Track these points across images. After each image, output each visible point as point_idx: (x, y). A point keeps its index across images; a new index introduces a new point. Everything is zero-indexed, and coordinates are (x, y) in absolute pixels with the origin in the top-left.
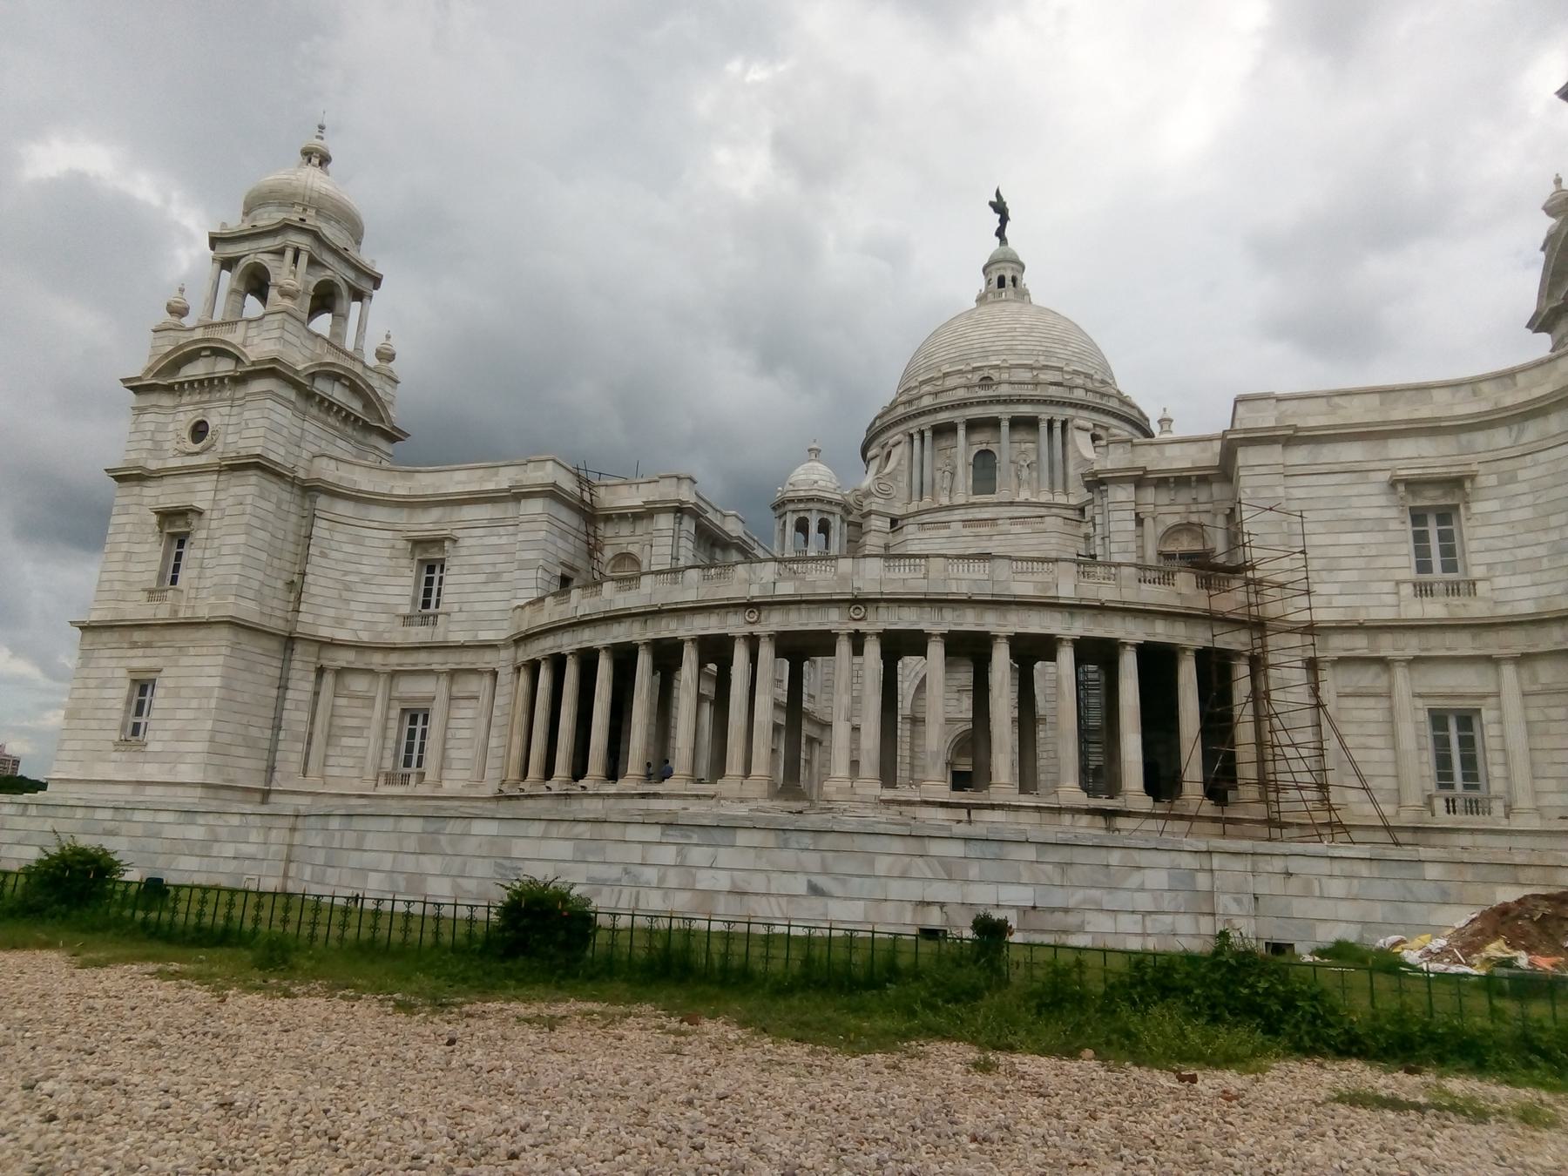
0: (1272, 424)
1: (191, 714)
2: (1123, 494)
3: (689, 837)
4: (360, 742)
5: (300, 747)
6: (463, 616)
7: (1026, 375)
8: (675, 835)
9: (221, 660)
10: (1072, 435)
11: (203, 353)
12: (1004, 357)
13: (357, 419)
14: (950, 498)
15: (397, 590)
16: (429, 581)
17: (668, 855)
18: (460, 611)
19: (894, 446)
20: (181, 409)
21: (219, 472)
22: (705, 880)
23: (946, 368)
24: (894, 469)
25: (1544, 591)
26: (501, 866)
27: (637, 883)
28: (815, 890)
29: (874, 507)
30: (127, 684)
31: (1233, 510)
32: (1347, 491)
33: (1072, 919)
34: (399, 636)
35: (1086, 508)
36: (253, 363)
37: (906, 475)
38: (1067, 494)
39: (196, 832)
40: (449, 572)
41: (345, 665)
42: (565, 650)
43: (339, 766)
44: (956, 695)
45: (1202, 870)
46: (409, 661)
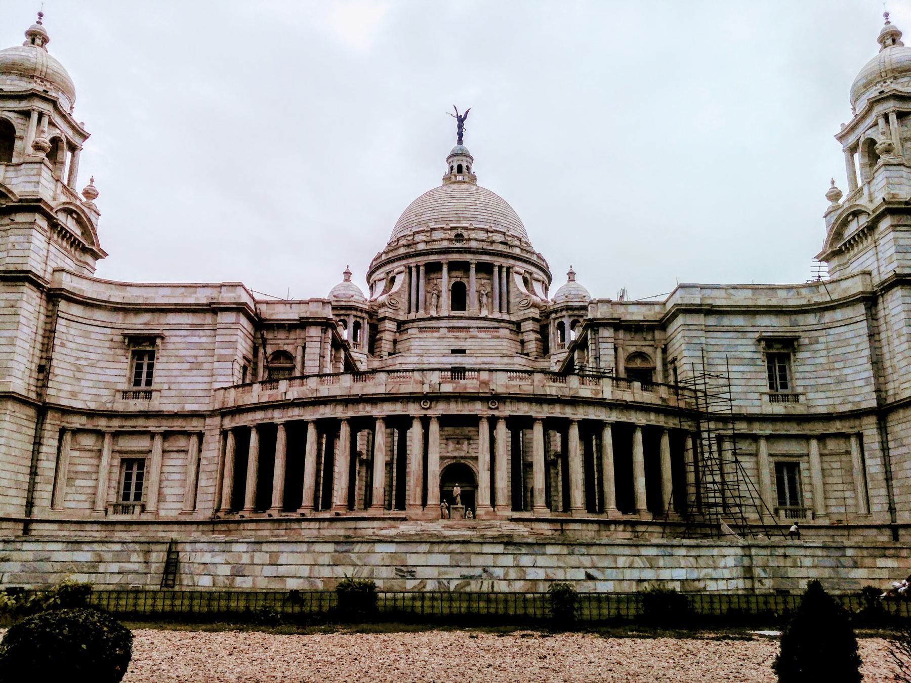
0: (699, 302)
2: (607, 333)
3: (520, 550)
4: (91, 483)
5: (50, 487)
6: (173, 393)
8: (511, 549)
10: (513, 277)
12: (471, 222)
13: (80, 242)
14: (437, 312)
16: (139, 367)
17: (508, 560)
18: (170, 389)
19: (397, 274)
22: (531, 574)
24: (400, 289)
25: (831, 401)
26: (401, 571)
28: (590, 577)
29: (388, 314)
31: (666, 345)
34: (120, 405)
35: (522, 324)
38: (508, 313)
39: (84, 556)
40: (158, 361)
41: (78, 426)
42: (276, 421)
44: (445, 441)
45: (745, 555)
46: (129, 424)
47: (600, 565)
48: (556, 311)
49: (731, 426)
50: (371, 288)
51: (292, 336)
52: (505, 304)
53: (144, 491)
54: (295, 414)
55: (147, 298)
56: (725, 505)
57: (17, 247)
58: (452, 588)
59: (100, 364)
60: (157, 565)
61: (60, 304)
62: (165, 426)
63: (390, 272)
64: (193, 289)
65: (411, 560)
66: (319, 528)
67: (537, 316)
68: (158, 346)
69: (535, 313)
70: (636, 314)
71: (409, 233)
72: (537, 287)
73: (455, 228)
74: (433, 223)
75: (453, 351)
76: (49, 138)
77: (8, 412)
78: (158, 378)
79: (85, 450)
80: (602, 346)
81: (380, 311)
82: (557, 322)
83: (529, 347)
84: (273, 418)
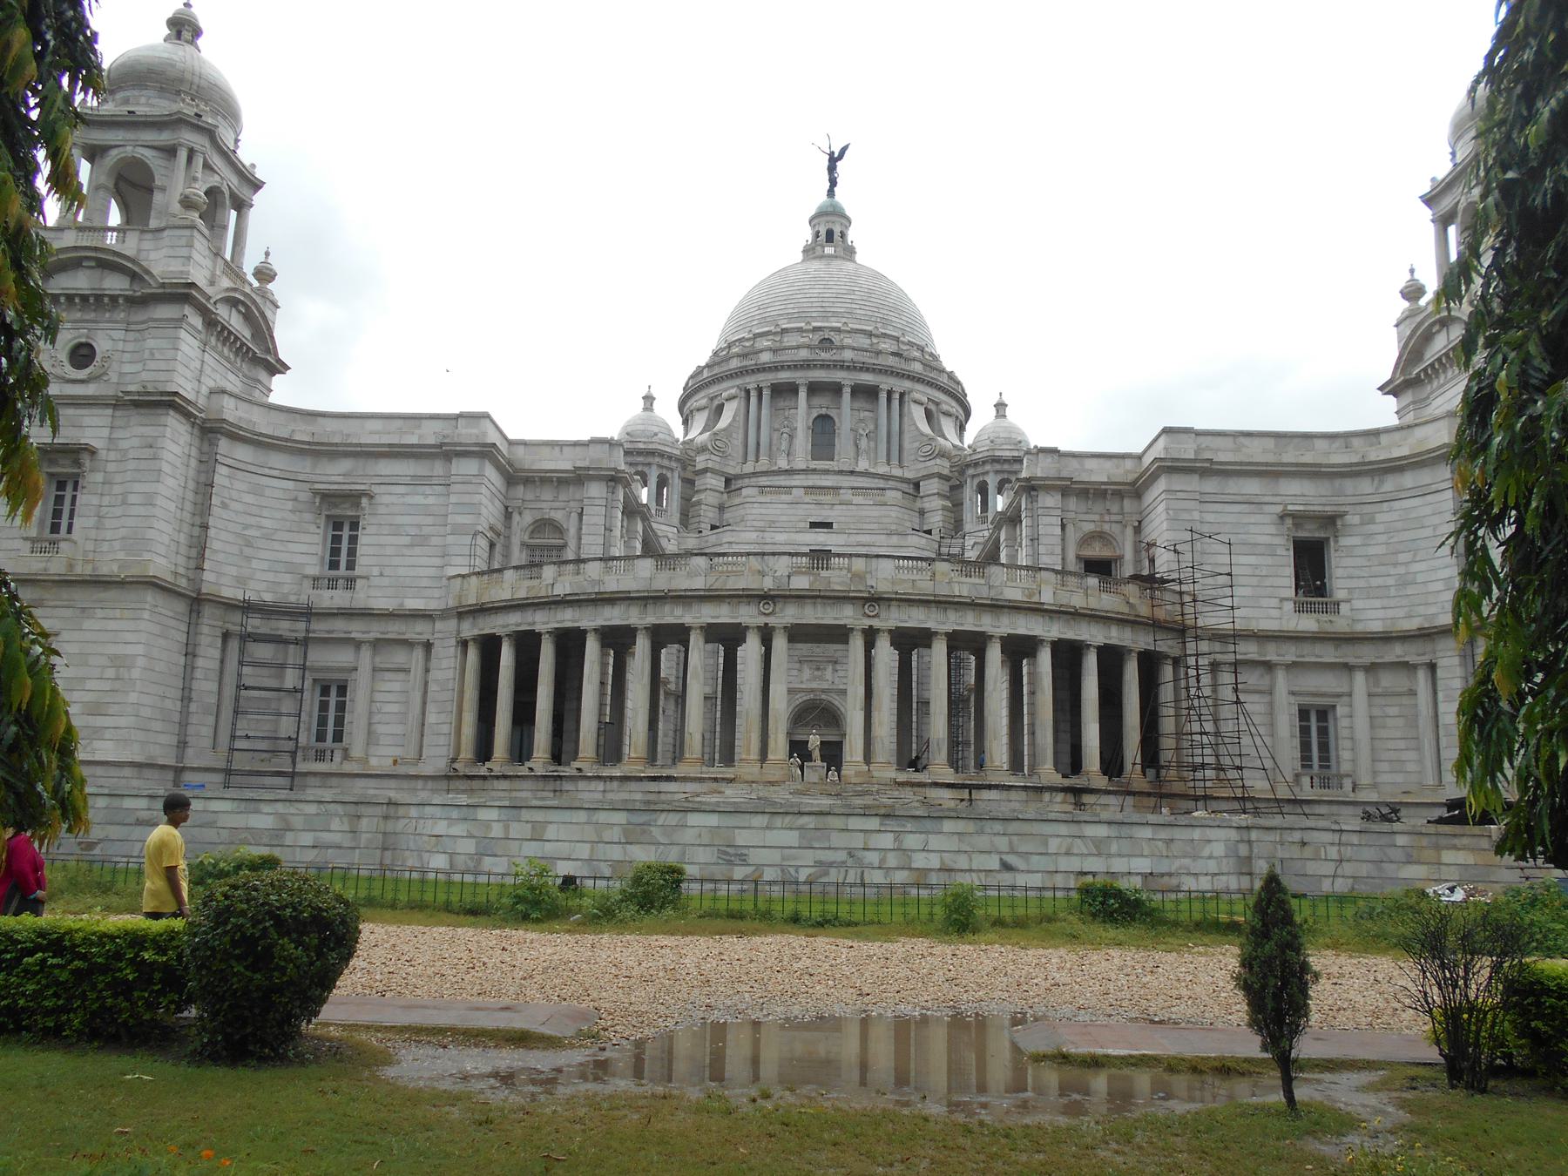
0: (1192, 457)
1: (107, 686)
2: (1050, 500)
5: (211, 720)
6: (385, 581)
7: (864, 342)
8: (892, 825)
13: (249, 349)
15: (304, 548)
16: (337, 539)
17: (887, 841)
18: (381, 575)
21: (115, 407)
22: (920, 861)
24: (730, 425)
25: (1390, 613)
27: (863, 866)
28: (1007, 867)
31: (1140, 522)
32: (1246, 519)
33: (1174, 881)
37: (741, 431)
38: (901, 467)
42: (538, 628)
44: (797, 665)
45: (1242, 841)
47: (1023, 849)
48: (976, 464)
49: (1231, 648)
50: (686, 422)
51: (562, 497)
52: (896, 452)
53: (346, 729)
54: (568, 618)
55: (348, 435)
56: (1219, 768)
57: (157, 356)
58: (802, 878)
60: (368, 835)
62: (376, 630)
64: (417, 422)
65: (742, 838)
66: (604, 791)
67: (946, 472)
68: (363, 509)
69: (943, 466)
70: (1098, 474)
71: (746, 335)
72: (948, 426)
73: (816, 329)
75: (814, 525)
76: (204, 189)
77: (147, 606)
78: (364, 560)
80: (1043, 520)
81: (698, 459)
82: (976, 481)
83: (932, 520)
84: (534, 623)
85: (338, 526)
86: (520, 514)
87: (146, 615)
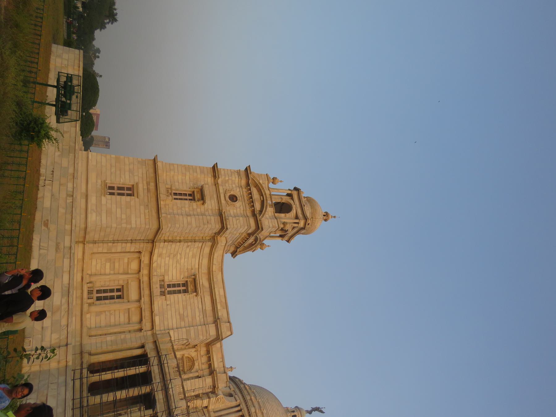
1: (119, 216)
4: (108, 271)
5: (106, 251)
9: (143, 226)
11: (261, 197)
18: (167, 305)
19: (235, 397)
20: (241, 189)
23: (265, 411)
30: (132, 183)
34: (155, 280)
36: (260, 220)
41: (142, 260)
43: (97, 264)
46: (145, 286)
53: (103, 302)
54: (159, 396)
57: (238, 221)
59: (178, 265)
61: (210, 242)
63: (235, 392)
68: (192, 293)
74: (265, 412)
79: (128, 265)
85: (184, 285)
86: (195, 351)
87: (147, 227)
